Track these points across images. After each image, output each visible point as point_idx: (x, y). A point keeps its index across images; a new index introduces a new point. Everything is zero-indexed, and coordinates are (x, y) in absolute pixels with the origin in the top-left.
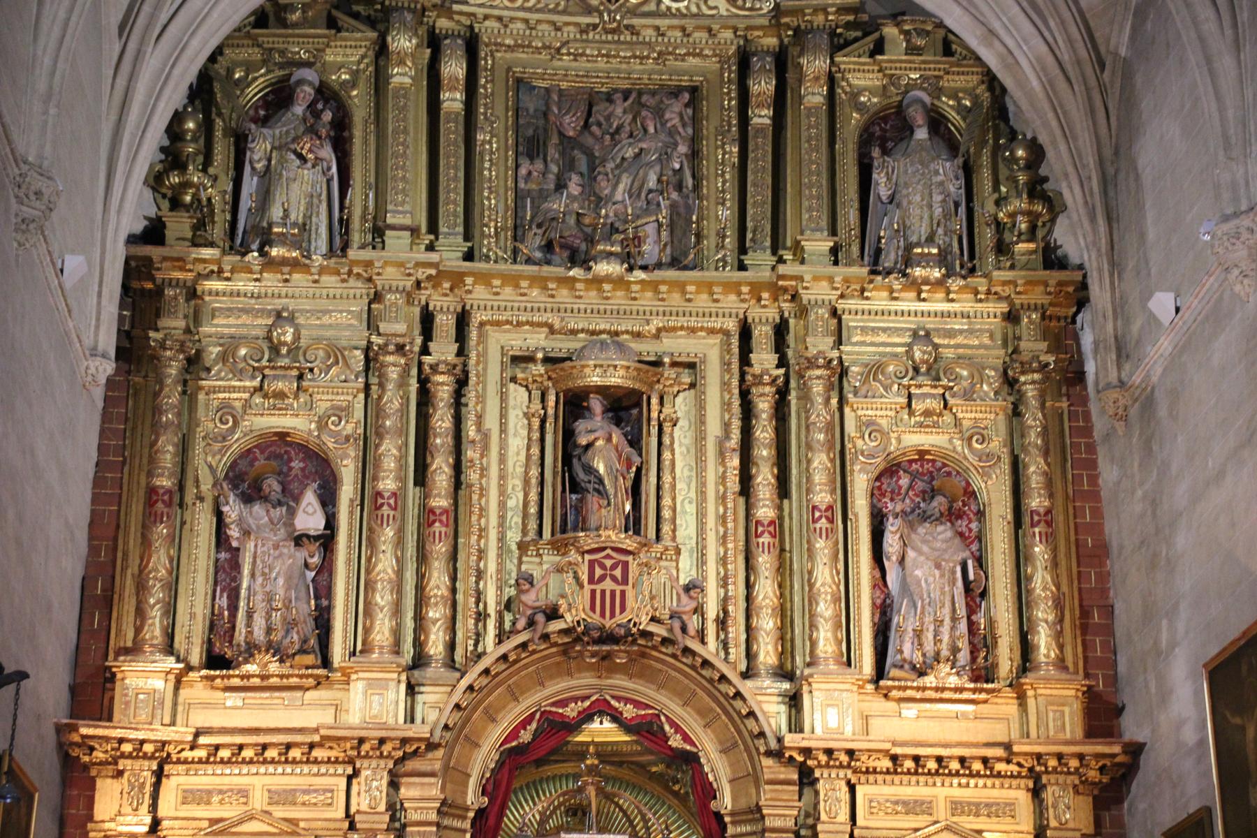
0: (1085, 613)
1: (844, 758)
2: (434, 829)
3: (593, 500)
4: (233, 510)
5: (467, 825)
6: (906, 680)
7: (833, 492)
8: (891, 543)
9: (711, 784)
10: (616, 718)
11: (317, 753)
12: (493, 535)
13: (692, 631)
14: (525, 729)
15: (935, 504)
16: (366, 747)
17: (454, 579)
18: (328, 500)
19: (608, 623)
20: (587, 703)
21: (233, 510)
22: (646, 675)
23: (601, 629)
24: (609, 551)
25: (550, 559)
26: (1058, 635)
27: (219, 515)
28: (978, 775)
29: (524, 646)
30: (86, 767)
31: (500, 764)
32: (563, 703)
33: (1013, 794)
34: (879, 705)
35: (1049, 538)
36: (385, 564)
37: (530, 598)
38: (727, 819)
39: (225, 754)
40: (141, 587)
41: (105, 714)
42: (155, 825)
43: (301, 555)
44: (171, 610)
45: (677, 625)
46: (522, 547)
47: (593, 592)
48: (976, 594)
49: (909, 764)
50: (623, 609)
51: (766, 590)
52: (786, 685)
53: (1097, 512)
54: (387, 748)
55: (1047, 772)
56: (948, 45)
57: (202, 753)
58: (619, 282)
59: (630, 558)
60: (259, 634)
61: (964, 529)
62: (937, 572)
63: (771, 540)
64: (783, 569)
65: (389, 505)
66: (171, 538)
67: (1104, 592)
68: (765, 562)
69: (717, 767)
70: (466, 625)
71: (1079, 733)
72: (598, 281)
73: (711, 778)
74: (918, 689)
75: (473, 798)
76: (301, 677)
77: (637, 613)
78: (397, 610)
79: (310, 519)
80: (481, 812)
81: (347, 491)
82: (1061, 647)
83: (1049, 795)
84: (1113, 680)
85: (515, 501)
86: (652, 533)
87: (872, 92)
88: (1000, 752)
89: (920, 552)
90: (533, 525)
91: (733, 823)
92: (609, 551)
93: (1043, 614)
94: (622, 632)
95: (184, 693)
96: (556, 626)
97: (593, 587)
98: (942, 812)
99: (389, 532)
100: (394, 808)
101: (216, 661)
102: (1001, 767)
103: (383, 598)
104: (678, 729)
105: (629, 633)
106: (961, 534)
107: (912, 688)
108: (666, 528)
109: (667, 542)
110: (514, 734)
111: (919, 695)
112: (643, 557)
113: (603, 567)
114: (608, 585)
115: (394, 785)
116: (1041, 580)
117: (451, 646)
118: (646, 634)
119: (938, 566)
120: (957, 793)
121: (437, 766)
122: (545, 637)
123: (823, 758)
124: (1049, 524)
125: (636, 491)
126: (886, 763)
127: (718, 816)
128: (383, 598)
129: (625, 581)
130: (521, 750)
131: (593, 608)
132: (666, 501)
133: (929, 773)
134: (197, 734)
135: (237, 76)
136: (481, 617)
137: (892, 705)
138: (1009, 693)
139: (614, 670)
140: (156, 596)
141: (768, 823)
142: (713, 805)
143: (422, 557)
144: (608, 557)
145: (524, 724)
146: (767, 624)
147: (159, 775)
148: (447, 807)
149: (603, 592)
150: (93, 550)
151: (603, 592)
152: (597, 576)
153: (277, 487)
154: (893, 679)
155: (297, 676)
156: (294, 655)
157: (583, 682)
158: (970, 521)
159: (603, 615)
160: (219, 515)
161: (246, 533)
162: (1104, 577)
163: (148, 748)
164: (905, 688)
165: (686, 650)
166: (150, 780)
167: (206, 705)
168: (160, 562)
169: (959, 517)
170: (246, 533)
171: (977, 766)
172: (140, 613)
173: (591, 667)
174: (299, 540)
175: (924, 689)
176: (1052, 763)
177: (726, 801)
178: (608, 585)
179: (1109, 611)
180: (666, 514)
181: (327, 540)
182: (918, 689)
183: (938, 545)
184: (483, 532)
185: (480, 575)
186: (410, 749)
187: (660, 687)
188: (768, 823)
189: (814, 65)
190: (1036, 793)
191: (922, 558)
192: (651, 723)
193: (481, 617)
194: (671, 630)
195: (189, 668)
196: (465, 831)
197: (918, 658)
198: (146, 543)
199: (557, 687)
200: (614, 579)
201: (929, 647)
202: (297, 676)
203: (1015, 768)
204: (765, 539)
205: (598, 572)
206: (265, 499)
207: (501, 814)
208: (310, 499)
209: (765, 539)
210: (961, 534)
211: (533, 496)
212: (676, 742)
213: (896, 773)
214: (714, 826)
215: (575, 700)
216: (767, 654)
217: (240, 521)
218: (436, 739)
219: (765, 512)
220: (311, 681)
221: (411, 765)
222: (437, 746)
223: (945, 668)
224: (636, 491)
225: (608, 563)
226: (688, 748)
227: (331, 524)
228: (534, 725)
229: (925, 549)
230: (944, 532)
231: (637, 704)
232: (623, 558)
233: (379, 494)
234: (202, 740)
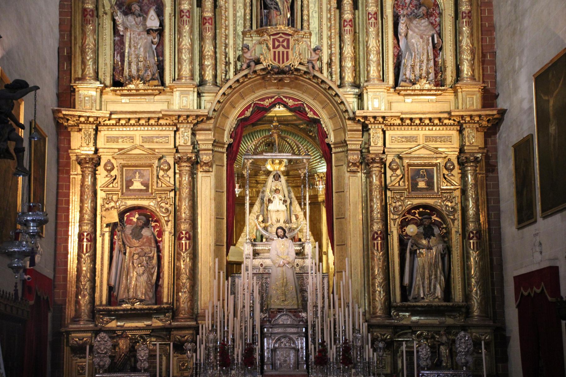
0: (484, 55)
1: (381, 120)
2: (211, 152)
3: (274, 12)
4: (120, 18)
5: (225, 150)
6: (407, 87)
7: (377, 6)
8: (402, 28)
9: (325, 132)
10: (285, 105)
11: (161, 122)
12: (231, 28)
13: (317, 68)
14: (247, 111)
15: (421, 10)
16: (181, 119)
17: (215, 48)
18: (160, 14)
19: (281, 66)
20: (273, 100)
21: (120, 18)
22: (298, 87)
23: (279, 68)
24: (281, 35)
25: (256, 38)
26: (472, 66)
27: (114, 21)
28: (437, 125)
29: (246, 76)
30: (66, 127)
31: (238, 125)
32: (263, 100)
33: (451, 132)
34: (396, 97)
35: (470, 24)
36: (186, 42)
37: (248, 55)
38: (332, 146)
39: (123, 122)
40: (83, 52)
41: (72, 106)
42: (96, 151)
43: (150, 38)
44: (96, 62)
45: (310, 66)
46: (244, 33)
47: (275, 52)
48: (437, 49)
49: (408, 122)
50: (287, 59)
51: (348, 50)
52: (357, 90)
53: (491, 12)
54: (190, 119)
55: (465, 123)
57: (113, 122)
59: (290, 37)
60: (134, 72)
61: (433, 21)
62: (421, 40)
63: (350, 28)
64: (355, 40)
65: (186, 16)
66: (94, 31)
67: (492, 46)
68: (348, 38)
69: (328, 125)
70: (221, 67)
71: (479, 107)
73: (325, 129)
74: (412, 90)
75: (227, 139)
76: (153, 90)
77: (294, 61)
78: (192, 61)
79: (153, 22)
80: (230, 145)
81: (168, 10)
82: (473, 71)
83: (466, 133)
84: (494, 84)
85: (240, 13)
86: (299, 27)
88: (446, 115)
89: (414, 32)
90: (248, 24)
91: (335, 147)
92: (281, 35)
93: (466, 56)
94: (287, 69)
95: (104, 97)
96: (259, 67)
97: (275, 50)
98: (421, 141)
99: (187, 28)
100: (194, 144)
101: (116, 83)
102: (446, 121)
103: (185, 56)
104: (311, 110)
105: (290, 70)
106: (432, 23)
107: (409, 90)
108: (305, 24)
109: (306, 30)
110: (243, 113)
111: (412, 93)
112: (296, 37)
113: (278, 41)
114: (281, 49)
115: (194, 134)
116: (465, 42)
117: (215, 76)
118: (297, 70)
119: (422, 38)
120: (428, 133)
121: (211, 126)
122: (255, 72)
123: (372, 120)
124: (470, 17)
125: (292, 8)
126: (399, 122)
127: (329, 145)
128: (185, 56)
129: (288, 47)
130: (246, 119)
131: (275, 59)
132: (305, 12)
133: (416, 125)
134: (111, 114)
136: (227, 64)
137: (401, 98)
138: (451, 91)
139: (284, 85)
140: (90, 56)
141: (349, 147)
142: (326, 141)
143: (202, 39)
144: (281, 37)
145: (247, 109)
146: (349, 64)
147: (96, 130)
148: (216, 143)
149: (279, 52)
150: (61, 36)
151: (279, 52)
152: (276, 46)
153: (138, 8)
154: (402, 86)
155: (151, 89)
156: (149, 80)
157: (272, 90)
158: (436, 17)
159: (279, 62)
160: (114, 21)
161: (126, 29)
162: (492, 40)
163: (91, 120)
164: (407, 90)
165: (315, 77)
166: (93, 132)
167: (114, 102)
168: (90, 41)
169: (431, 16)
170: (126, 29)
171: (436, 121)
172: (84, 63)
173: (274, 85)
174: (149, 31)
175: (415, 90)
176: (468, 119)
177: (332, 139)
178: (281, 49)
179: (494, 54)
180: (305, 18)
181: (161, 31)
182: (412, 90)
183: (422, 28)
184: (227, 27)
185: (226, 46)
186: (200, 119)
187: (304, 92)
188: (349, 147)
190: (461, 131)
191: (415, 34)
192: (300, 107)
193: (227, 64)
194: (308, 68)
195: (106, 86)
196: (223, 153)
197: (412, 77)
198: (84, 33)
199: (260, 93)
200: (283, 46)
201: (417, 72)
202: (151, 89)
203: (452, 122)
204: (348, 28)
205: (277, 44)
206: (133, 14)
207: (238, 146)
208: (152, 13)
209: (348, 28)
210: (432, 23)
211: (248, 11)
212: (311, 115)
213: (402, 125)
214: (327, 148)
215: (268, 98)
216: (349, 77)
217: (123, 23)
218: (210, 115)
219: (347, 16)
220: (157, 92)
221: (200, 126)
222: (211, 118)
223: (424, 81)
224: (292, 8)
225: (281, 40)
226: (316, 117)
227: (162, 24)
228: (251, 109)
229: (416, 30)
230: (425, 22)
231: (294, 100)
232: (287, 37)
233: (182, 11)
234: (113, 116)
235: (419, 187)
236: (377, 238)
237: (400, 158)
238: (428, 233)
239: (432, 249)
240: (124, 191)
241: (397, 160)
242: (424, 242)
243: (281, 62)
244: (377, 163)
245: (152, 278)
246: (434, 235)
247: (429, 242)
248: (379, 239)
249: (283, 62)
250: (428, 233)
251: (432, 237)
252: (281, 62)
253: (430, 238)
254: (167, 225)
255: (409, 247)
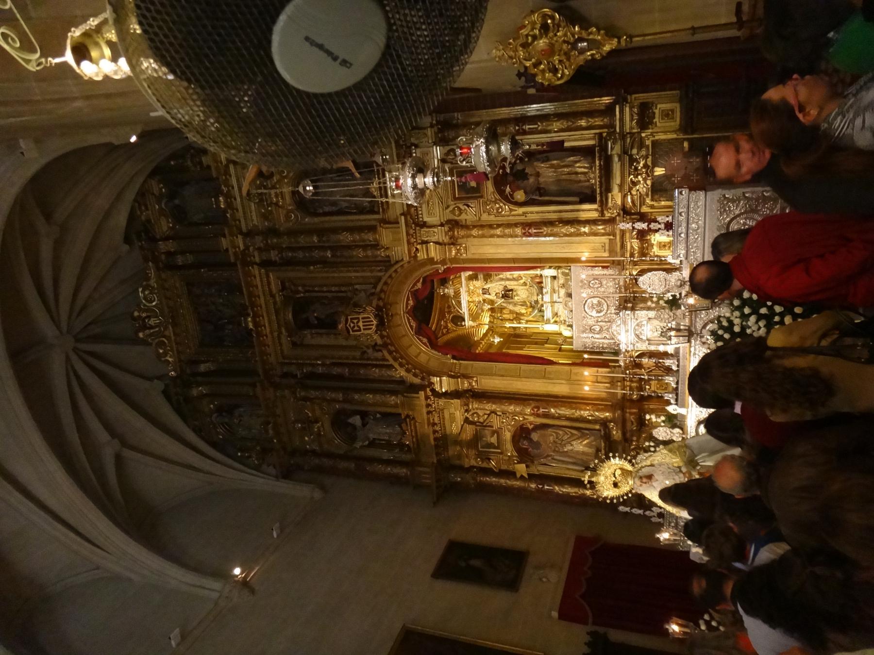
4: (358, 445)
19: (375, 322)
20: (410, 318)
23: (377, 326)
24: (348, 325)
32: (411, 327)
38: (445, 267)
47: (364, 329)
56: (142, 194)
58: (254, 318)
59: (349, 317)
72: (256, 324)
87: (168, 222)
92: (348, 325)
110: (425, 344)
113: (354, 327)
131: (371, 329)
135: (221, 437)
144: (350, 325)
159: (373, 325)
178: (361, 324)
189: (162, 246)
200: (358, 322)
204: (339, 254)
205: (356, 328)
208: (350, 420)
212: (419, 285)
225: (352, 325)
226: (421, 281)
231: (408, 299)
235: (475, 186)
236: (529, 233)
237: (448, 207)
238: (521, 176)
239: (539, 172)
240: (500, 451)
241: (451, 208)
242: (532, 180)
243: (372, 323)
244: (454, 232)
245: (577, 435)
246: (524, 170)
247: (531, 175)
248: (530, 231)
249: (372, 321)
250: (521, 176)
251: (526, 171)
252: (372, 323)
253: (528, 173)
254: (527, 419)
255: (537, 198)
